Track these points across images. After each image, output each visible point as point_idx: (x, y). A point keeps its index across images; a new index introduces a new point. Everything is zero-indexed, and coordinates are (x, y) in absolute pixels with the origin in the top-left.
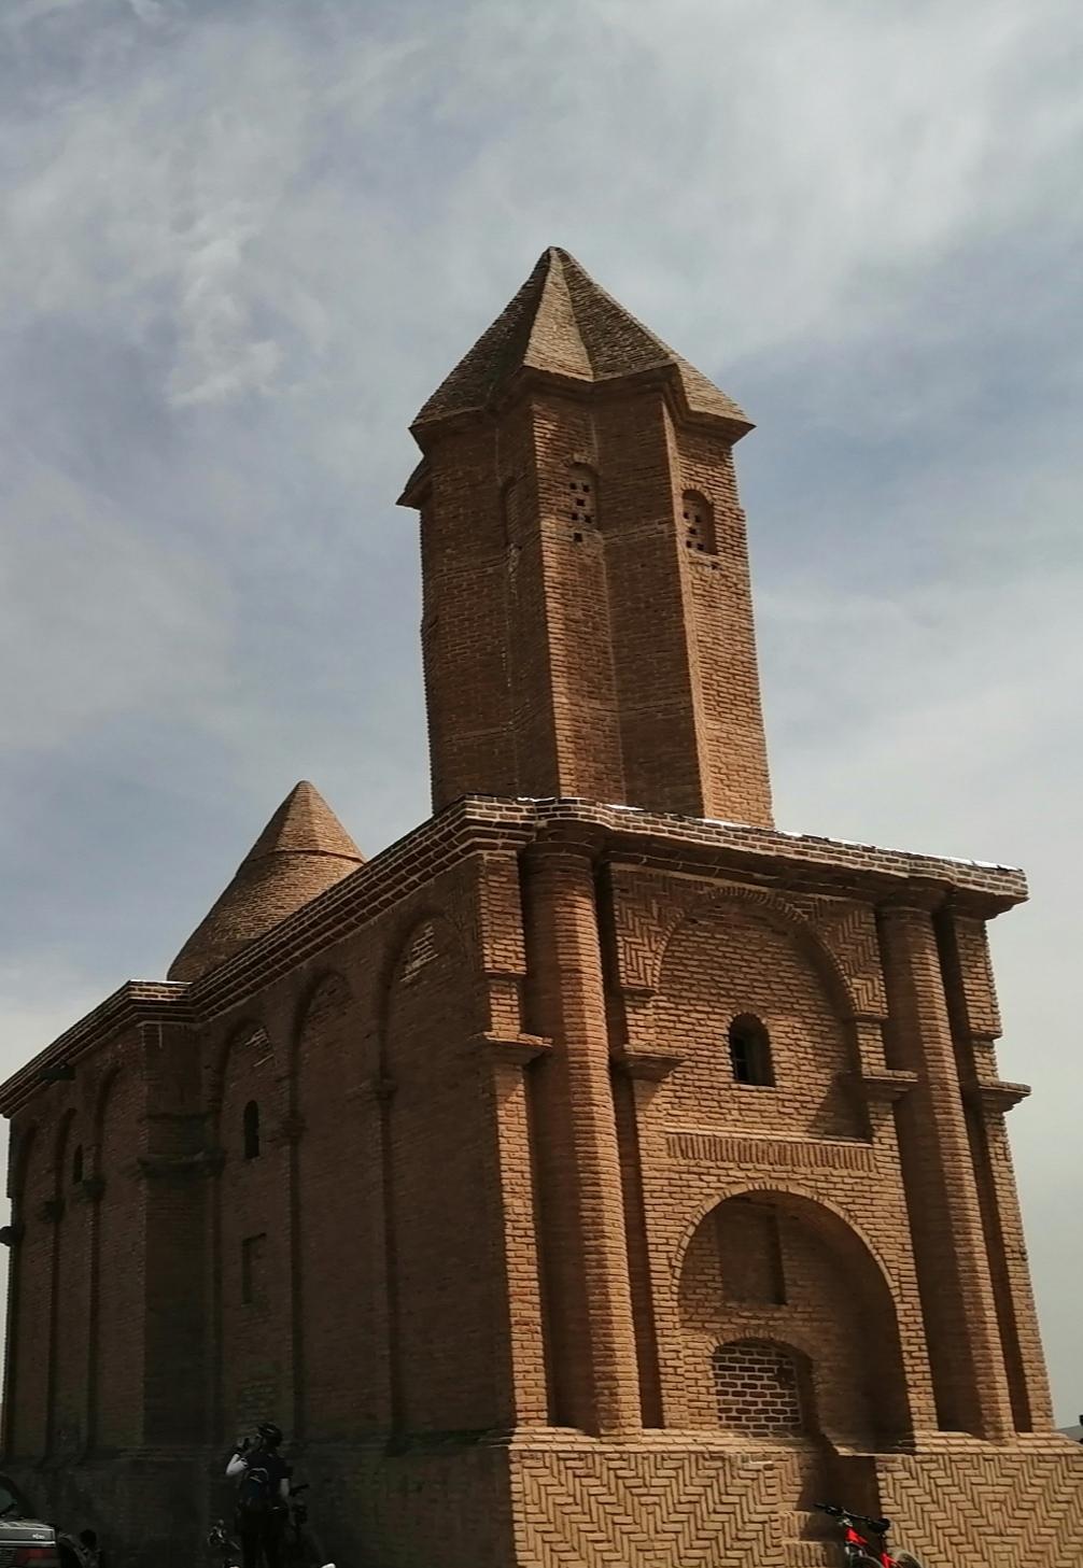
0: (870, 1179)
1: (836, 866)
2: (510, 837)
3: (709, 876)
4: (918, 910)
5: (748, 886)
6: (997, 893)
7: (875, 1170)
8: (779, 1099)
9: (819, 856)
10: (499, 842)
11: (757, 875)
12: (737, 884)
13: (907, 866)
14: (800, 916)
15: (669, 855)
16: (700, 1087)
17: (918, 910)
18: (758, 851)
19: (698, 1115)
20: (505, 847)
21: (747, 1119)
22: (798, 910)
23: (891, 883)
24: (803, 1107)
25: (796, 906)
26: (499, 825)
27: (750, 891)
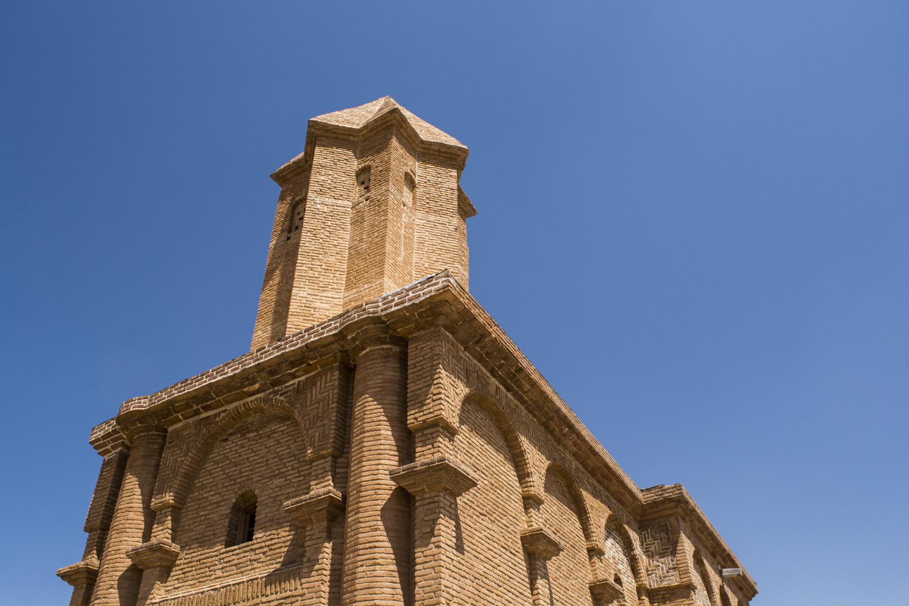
0: (293, 596)
1: (282, 355)
2: (114, 440)
3: (222, 405)
4: (368, 350)
5: (249, 399)
6: (417, 301)
7: (300, 587)
8: (252, 550)
9: (272, 354)
10: (109, 447)
11: (246, 389)
12: (241, 402)
13: (338, 324)
14: (282, 401)
15: (188, 406)
16: (199, 560)
17: (368, 350)
18: (231, 374)
19: (191, 583)
20: (113, 448)
21: (226, 574)
22: (282, 398)
23: (332, 343)
24: (271, 550)
25: (281, 395)
26: (104, 437)
27: (251, 402)
